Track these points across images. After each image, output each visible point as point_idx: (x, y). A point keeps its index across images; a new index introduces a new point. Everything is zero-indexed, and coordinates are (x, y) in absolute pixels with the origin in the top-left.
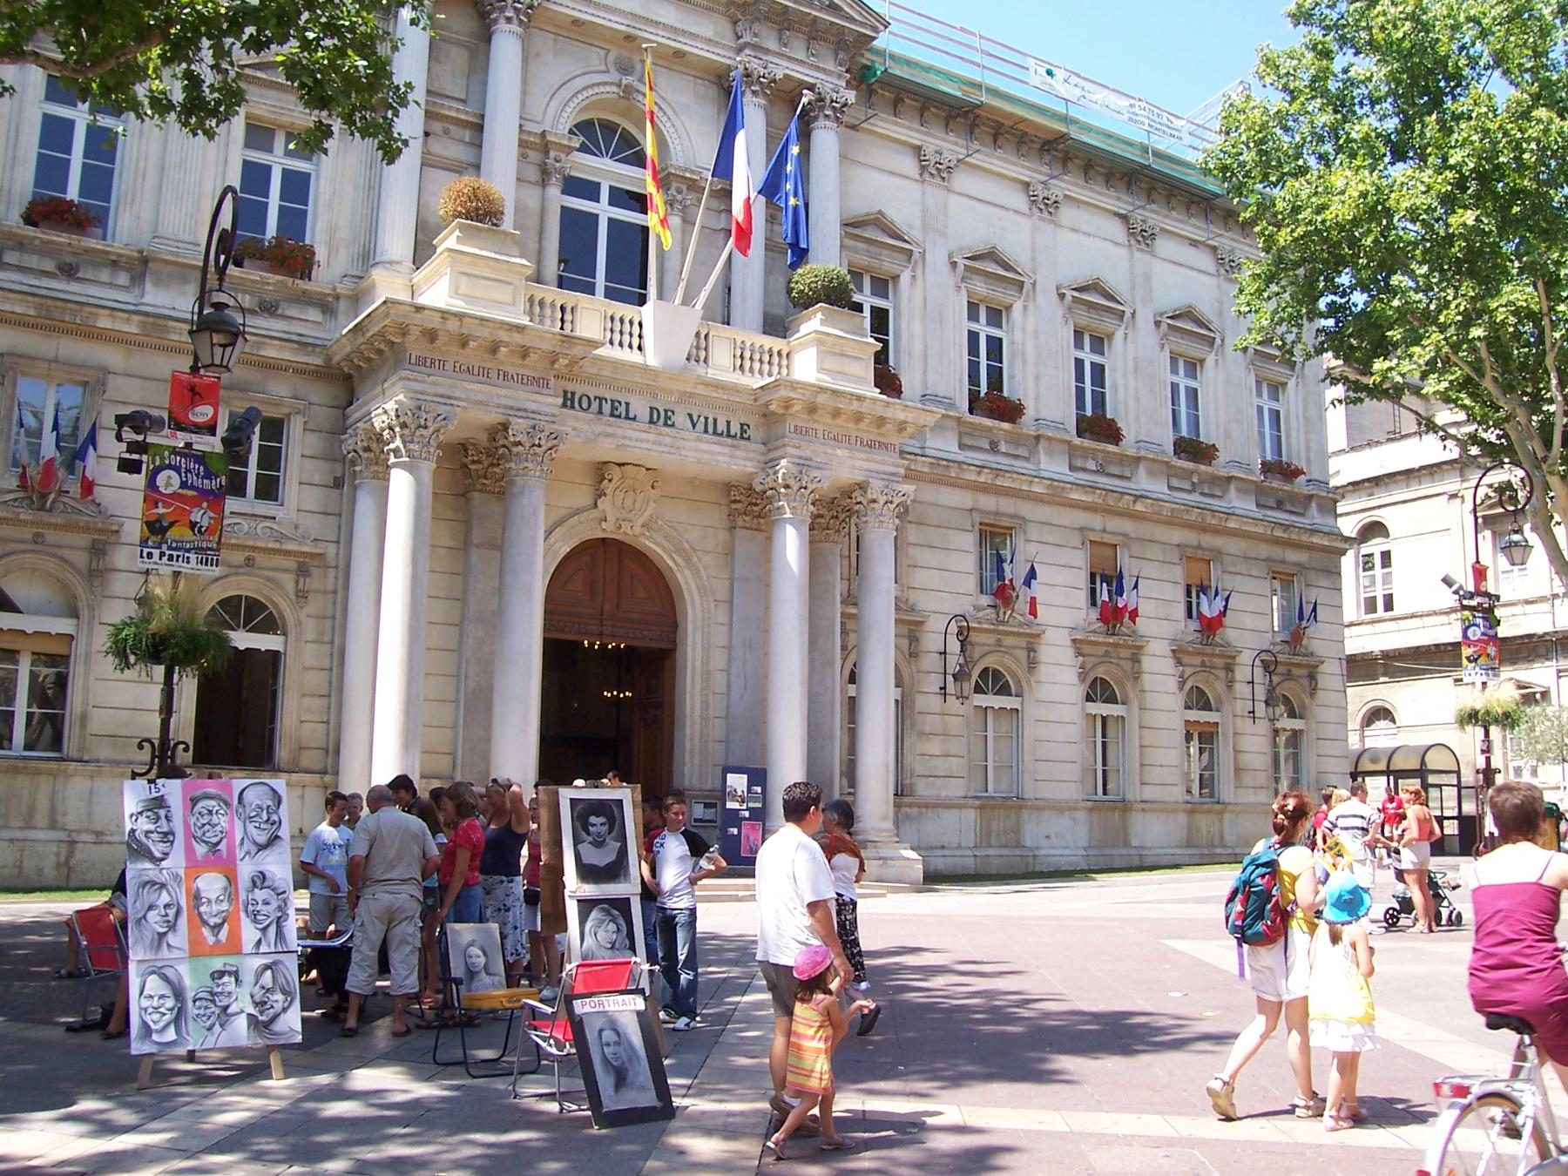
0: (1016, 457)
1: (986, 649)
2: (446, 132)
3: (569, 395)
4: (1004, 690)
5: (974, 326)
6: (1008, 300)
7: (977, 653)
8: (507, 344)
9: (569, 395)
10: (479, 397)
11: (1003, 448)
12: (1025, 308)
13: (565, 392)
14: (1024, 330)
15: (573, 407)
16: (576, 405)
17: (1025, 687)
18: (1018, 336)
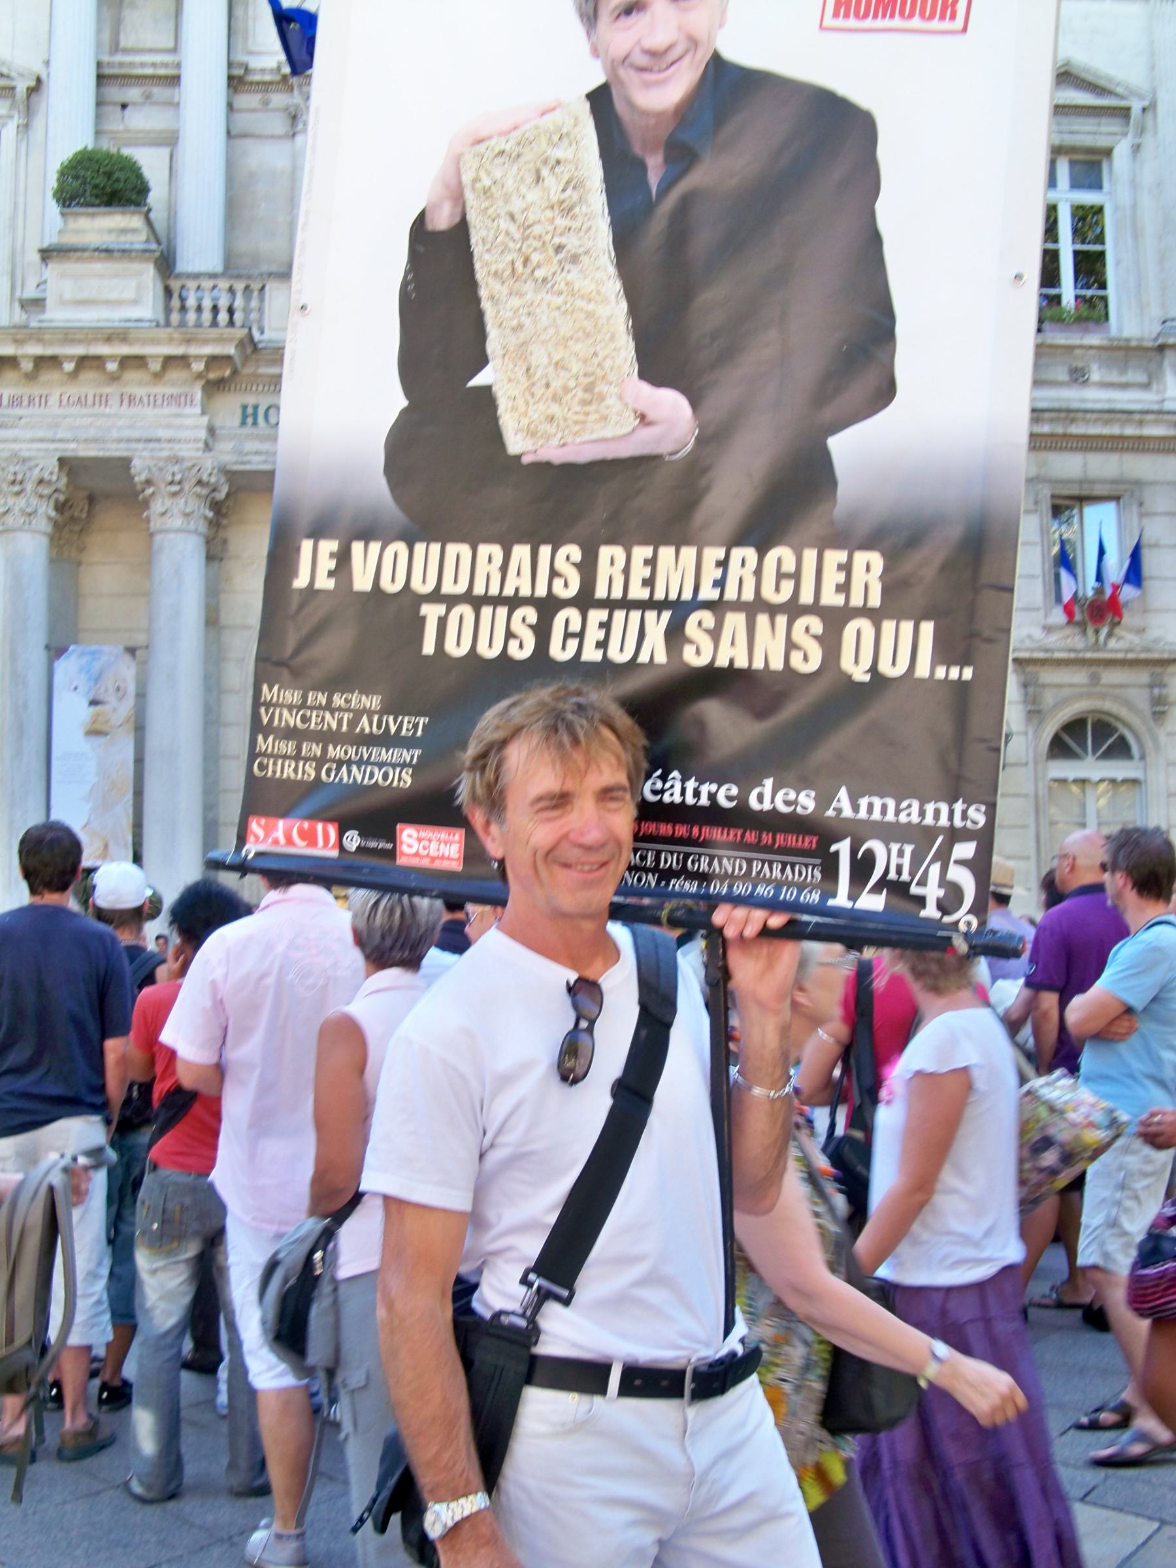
0: (1125, 386)
1: (1066, 692)
2: (148, 97)
3: (250, 411)
4: (1120, 749)
5: (1053, 196)
6: (1102, 142)
7: (1049, 698)
8: (112, 358)
9: (250, 411)
10: (92, 433)
11: (1096, 375)
12: (1136, 149)
13: (245, 408)
14: (1134, 184)
15: (255, 423)
16: (261, 419)
17: (1149, 744)
18: (1124, 195)
